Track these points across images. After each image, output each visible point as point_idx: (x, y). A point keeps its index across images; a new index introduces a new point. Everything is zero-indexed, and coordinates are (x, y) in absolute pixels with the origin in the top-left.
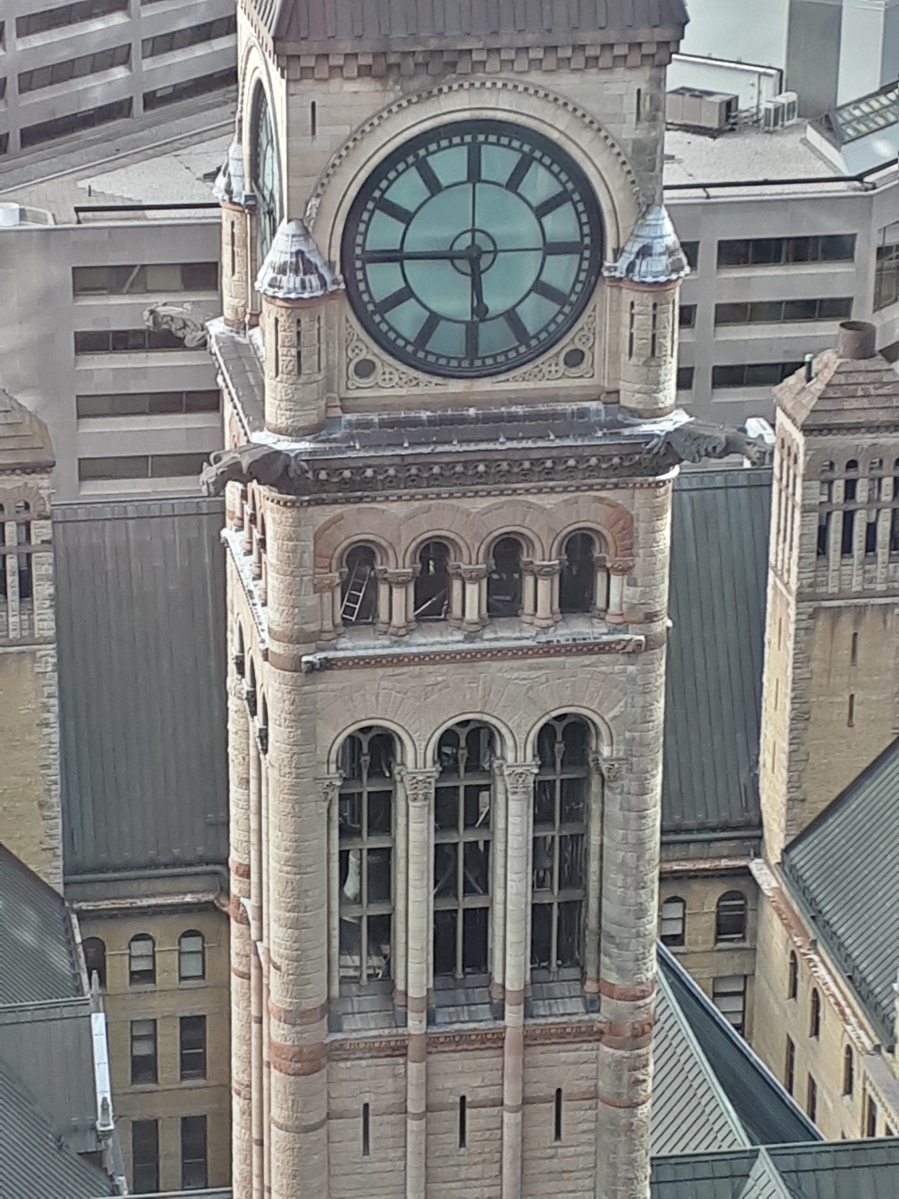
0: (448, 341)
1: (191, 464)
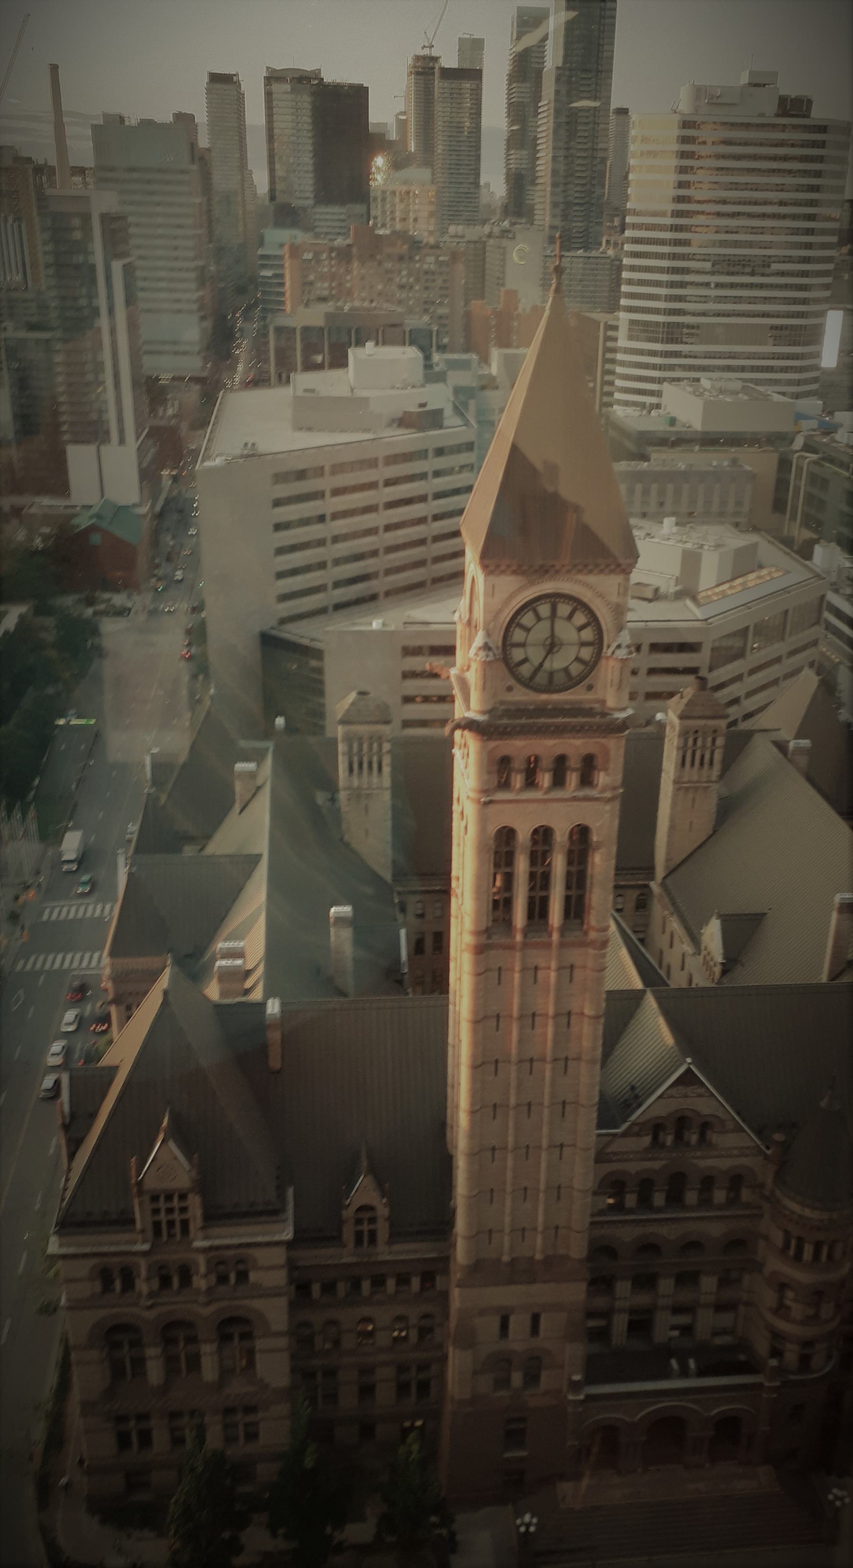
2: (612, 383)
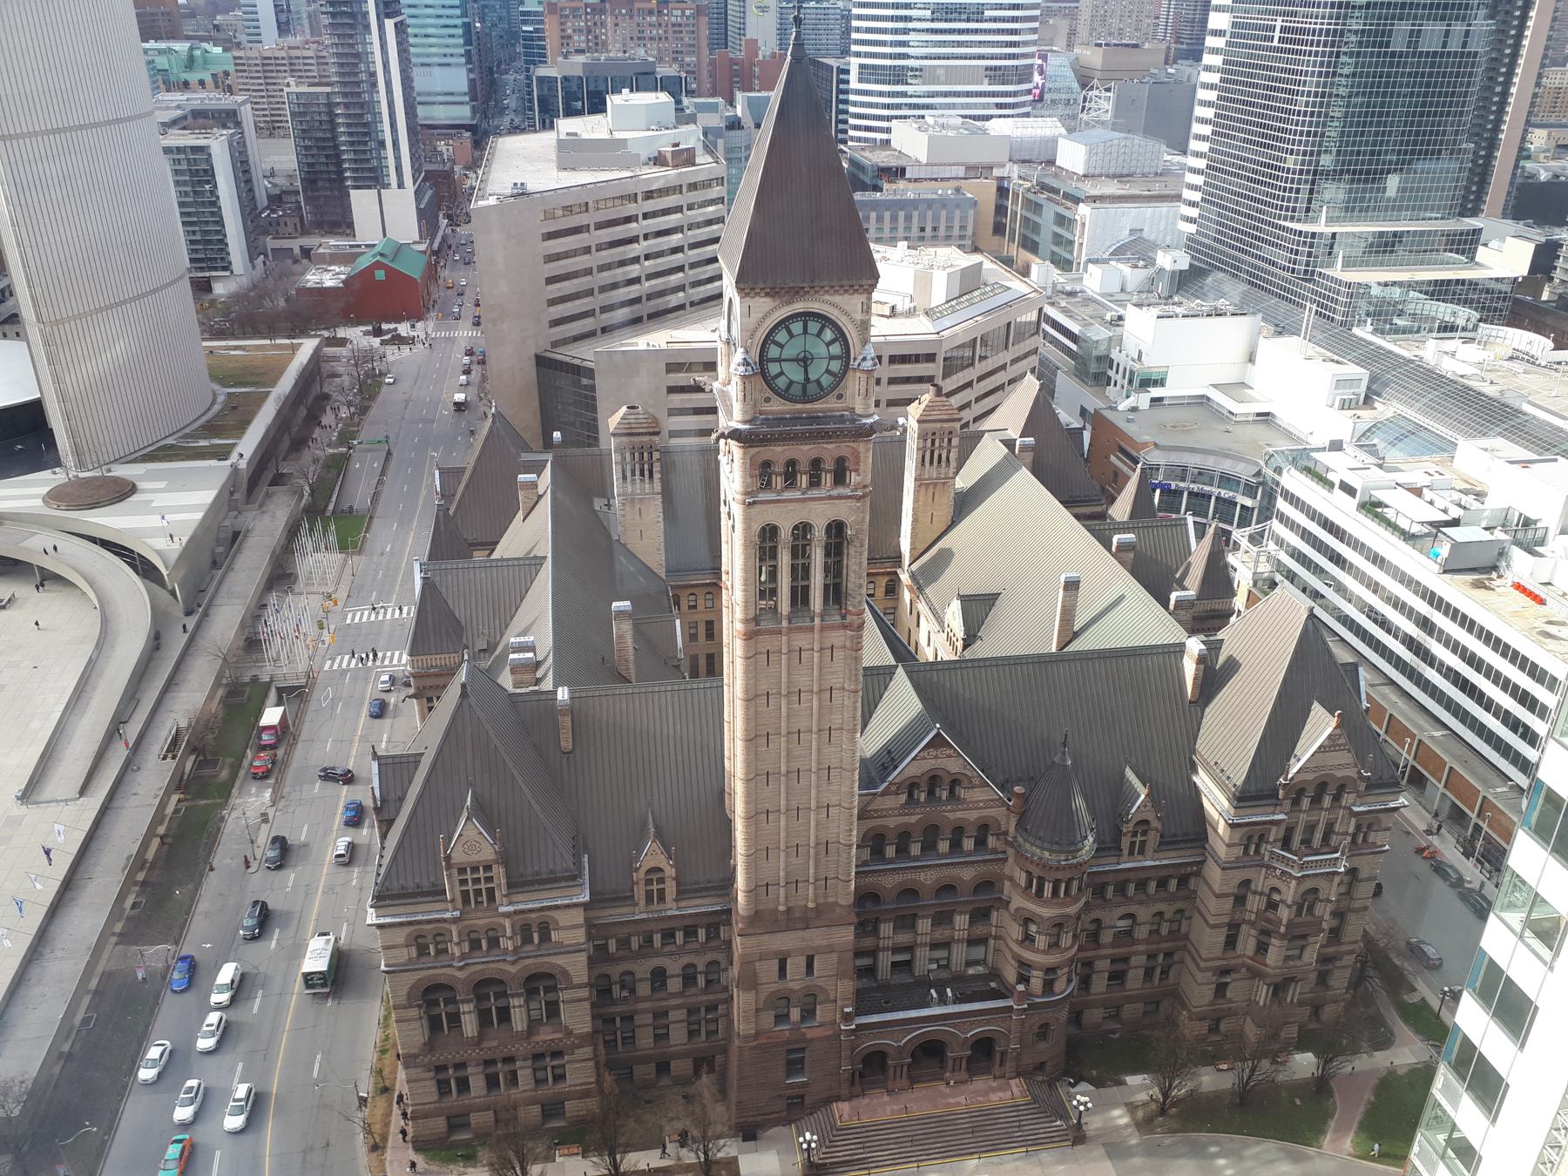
0: (796, 390)
1: (706, 433)
2: (846, 122)
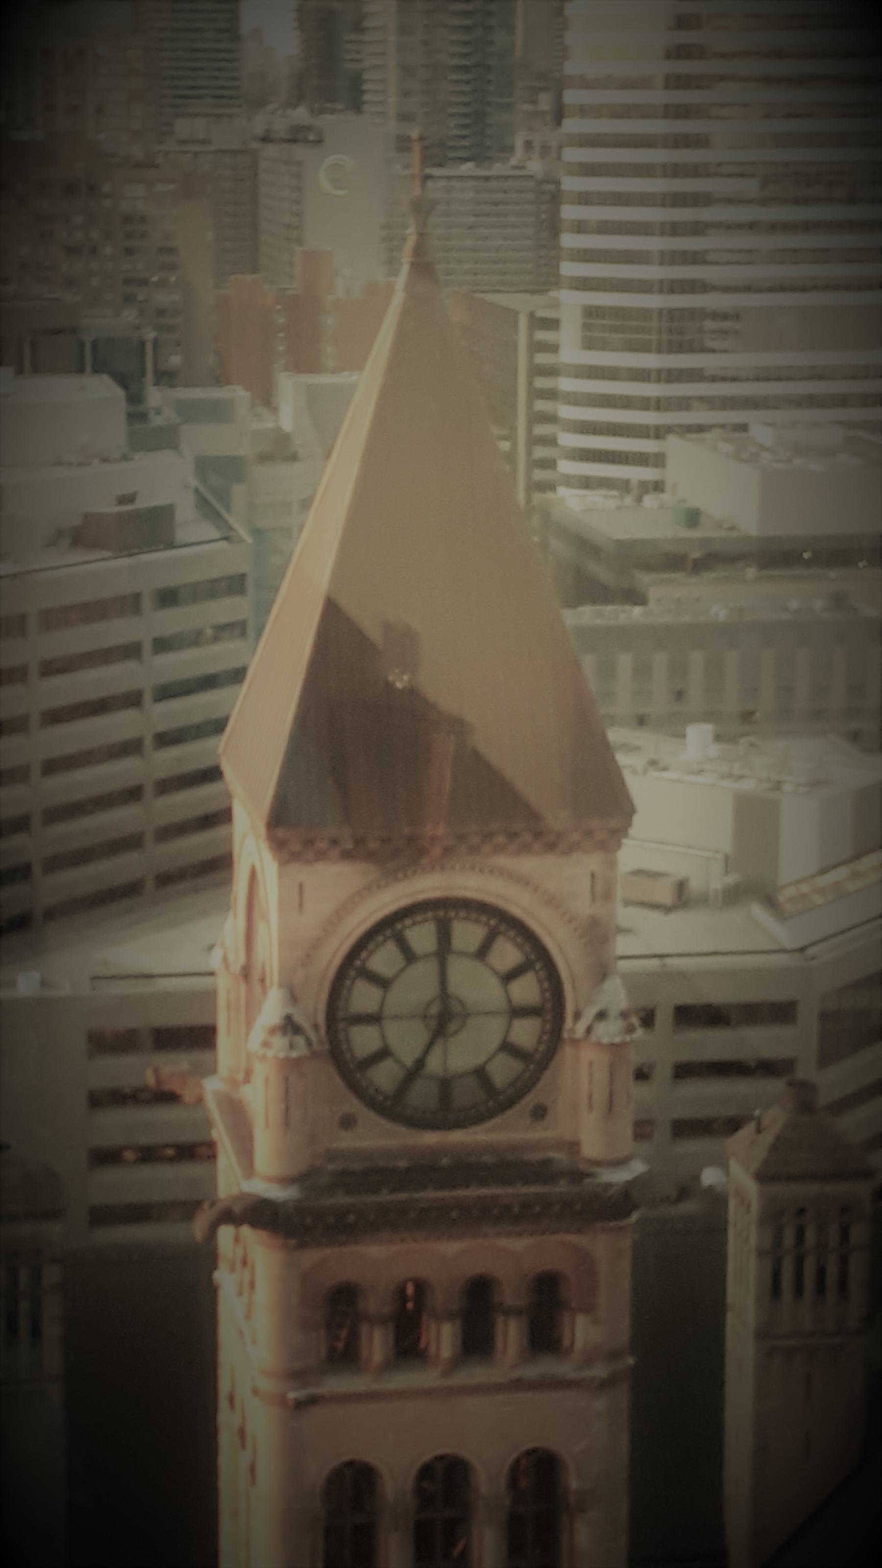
2: (550, 441)
